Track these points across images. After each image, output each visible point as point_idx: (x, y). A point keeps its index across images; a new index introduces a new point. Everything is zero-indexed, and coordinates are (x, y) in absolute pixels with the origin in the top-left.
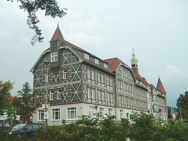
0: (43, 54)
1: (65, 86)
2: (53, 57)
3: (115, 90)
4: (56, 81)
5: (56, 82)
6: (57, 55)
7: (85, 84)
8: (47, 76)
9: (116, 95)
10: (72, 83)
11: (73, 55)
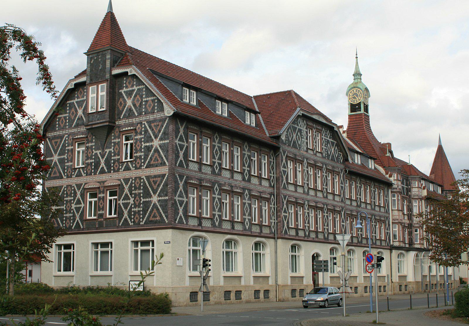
0: (70, 87)
1: (127, 180)
3: (278, 189)
4: (103, 164)
5: (103, 168)
6: (104, 93)
10: (144, 173)
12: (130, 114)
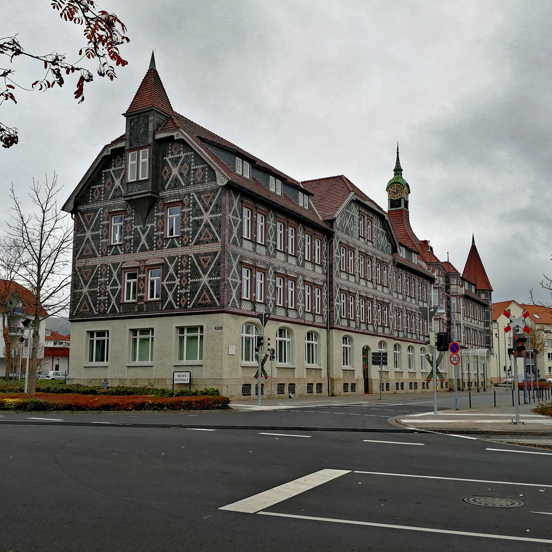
0: (105, 153)
1: (172, 259)
2: (137, 167)
3: (331, 276)
4: (143, 241)
5: (143, 245)
6: (147, 160)
7: (235, 255)
8: (116, 224)
9: (331, 290)
10: (192, 250)
11: (199, 159)
12: (176, 184)
